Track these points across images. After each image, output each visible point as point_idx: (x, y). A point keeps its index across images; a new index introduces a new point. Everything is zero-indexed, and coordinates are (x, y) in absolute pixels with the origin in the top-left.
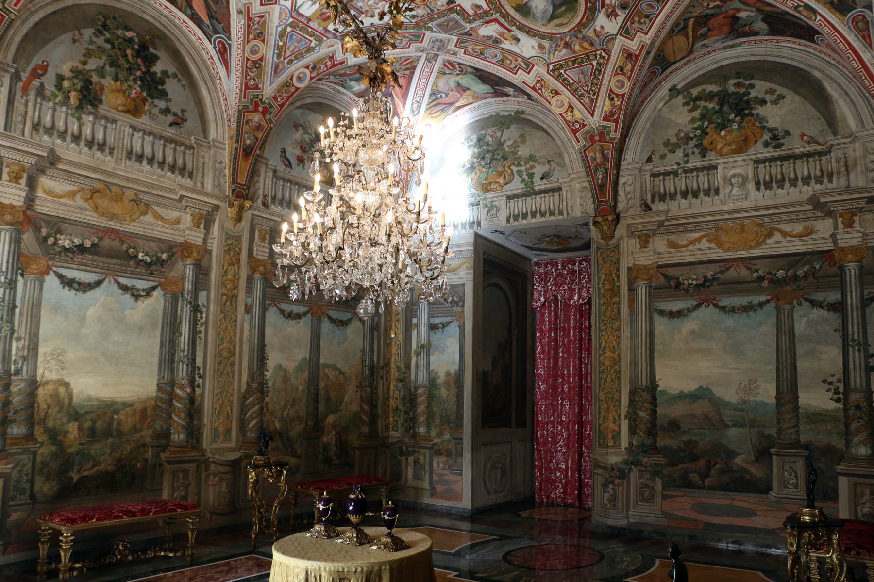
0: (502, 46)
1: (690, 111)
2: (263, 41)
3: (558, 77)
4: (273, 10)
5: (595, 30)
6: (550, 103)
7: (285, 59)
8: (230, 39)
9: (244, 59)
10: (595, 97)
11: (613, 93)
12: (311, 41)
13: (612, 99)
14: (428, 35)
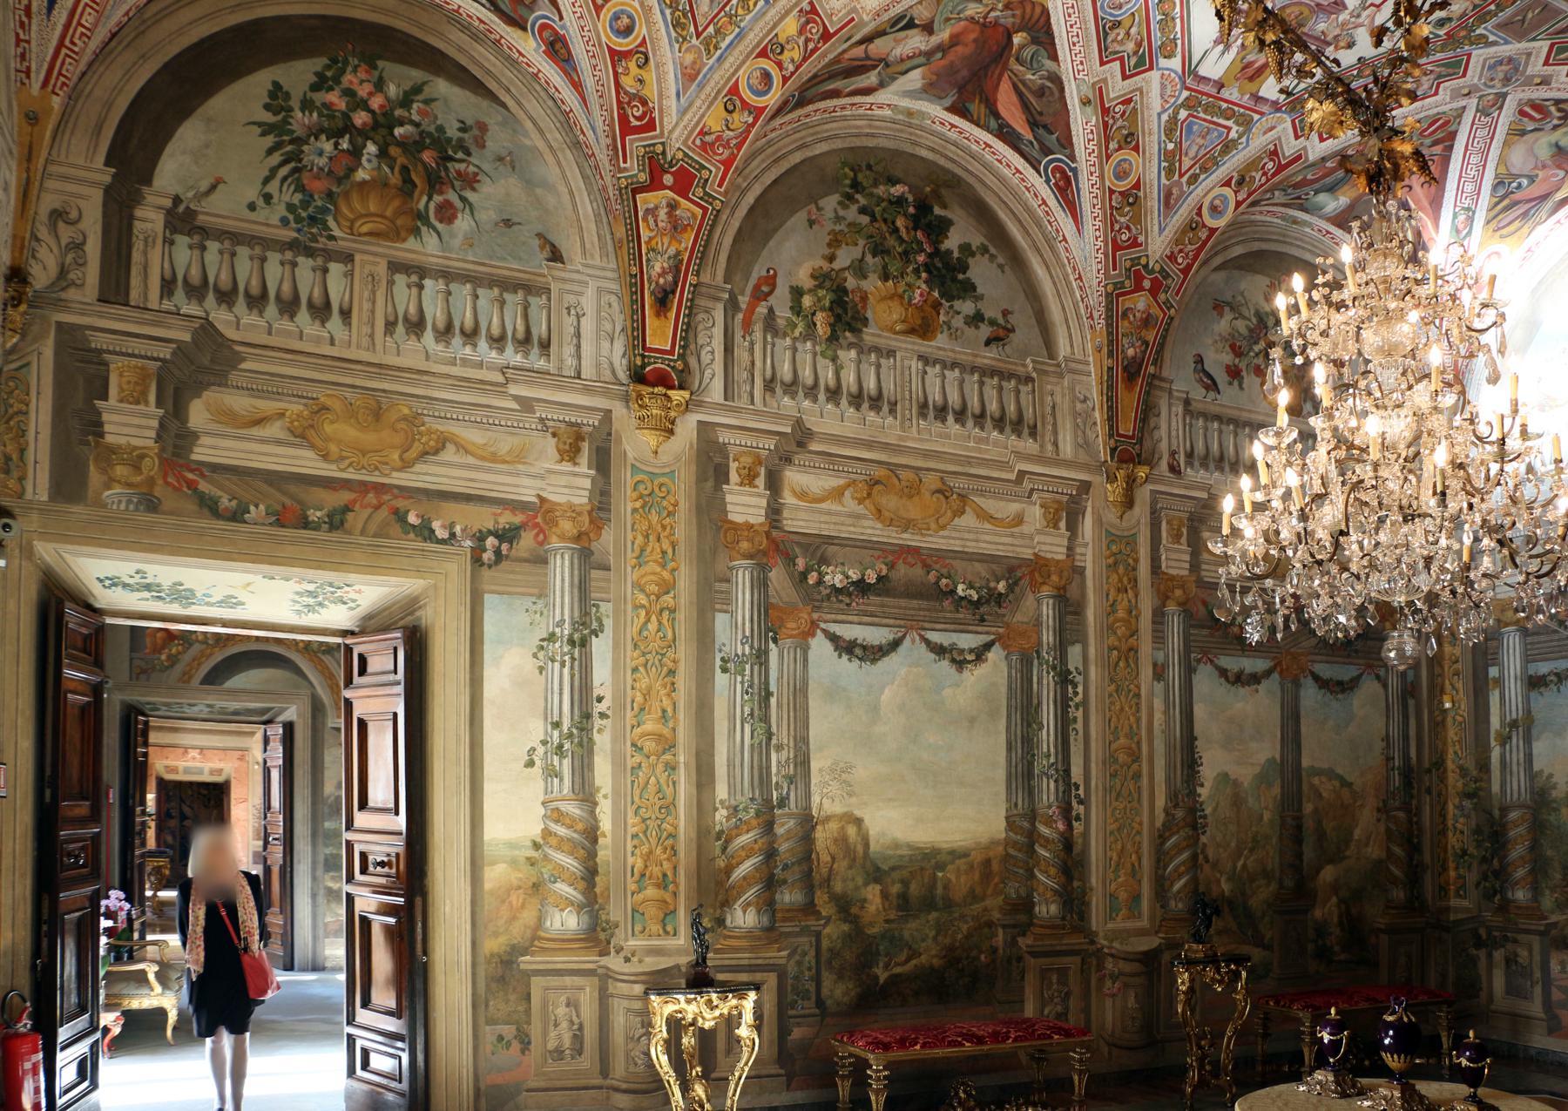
2: (1136, 149)
4: (1147, 82)
7: (1181, 176)
8: (1072, 158)
12: (1229, 129)
14: (1479, 55)
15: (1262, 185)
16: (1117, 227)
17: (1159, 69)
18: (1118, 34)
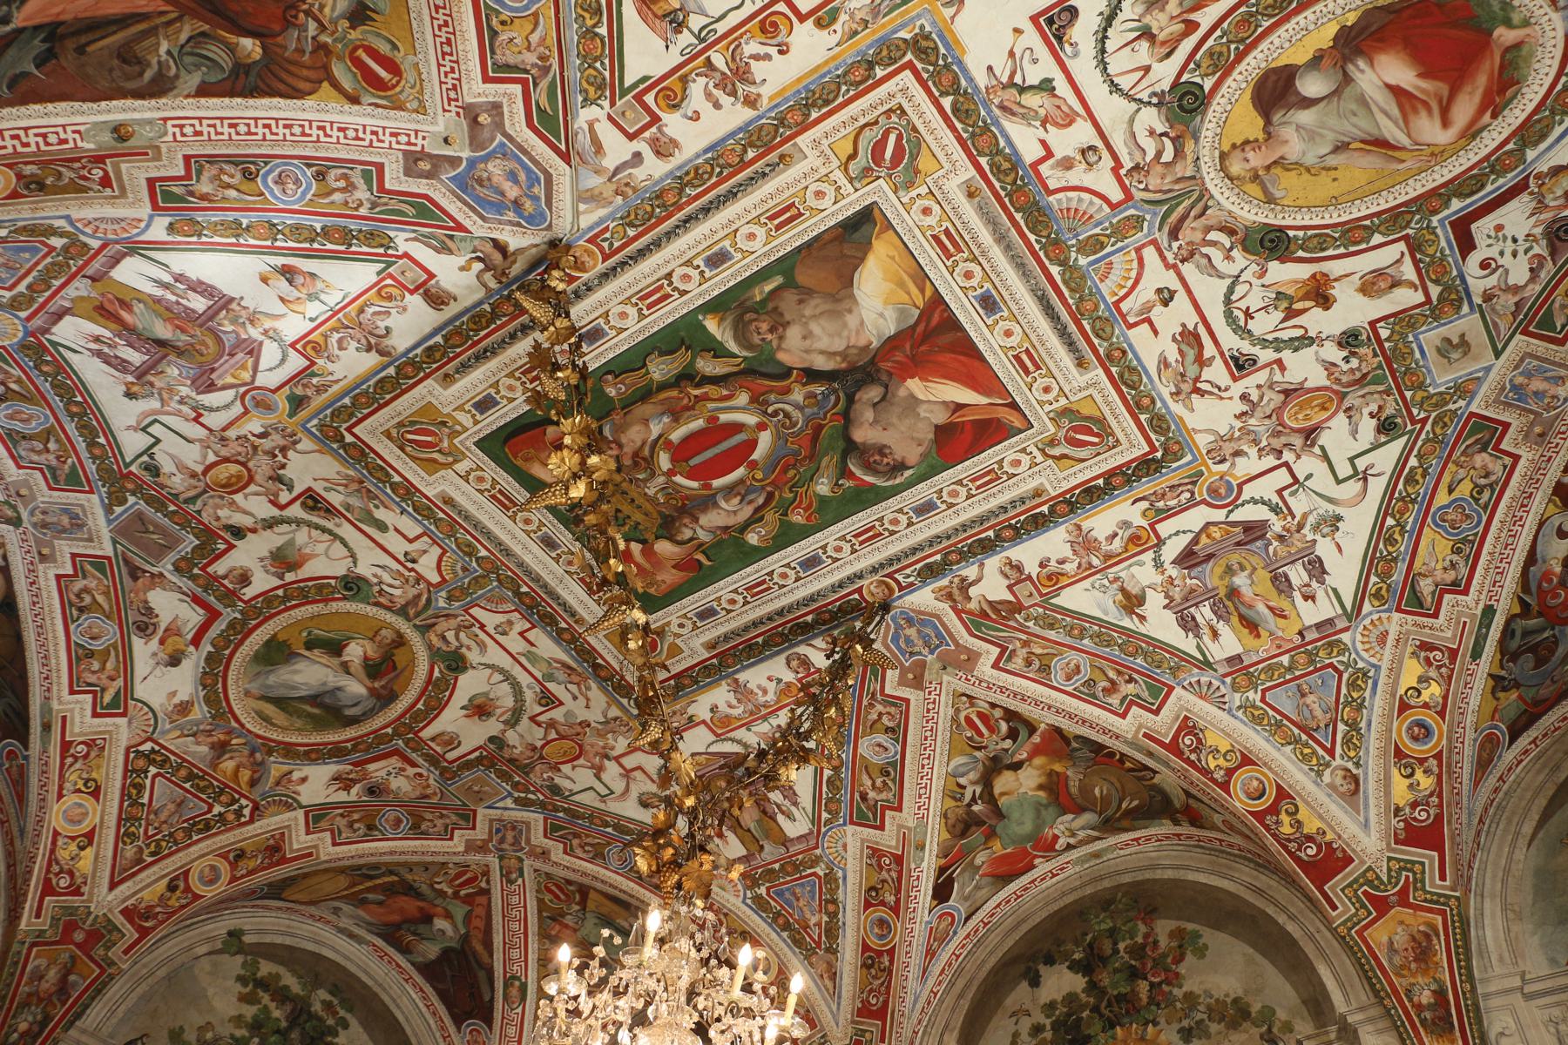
0: (137, 643)
1: (243, 999)
3: (134, 771)
6: (60, 796)
10: (150, 859)
11: (186, 880)
13: (172, 888)
17: (151, 217)
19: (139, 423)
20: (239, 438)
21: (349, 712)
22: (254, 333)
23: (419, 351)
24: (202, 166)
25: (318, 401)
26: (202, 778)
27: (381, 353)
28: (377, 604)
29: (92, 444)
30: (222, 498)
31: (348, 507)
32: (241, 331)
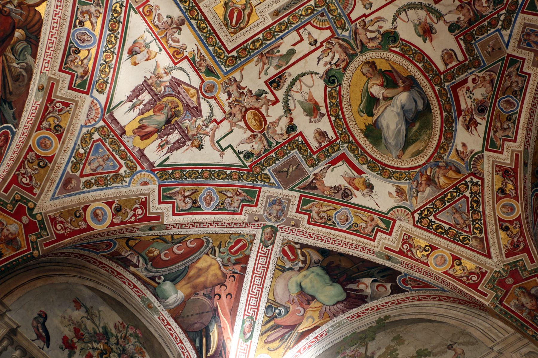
0: (354, 200)
2: (60, 137)
3: (428, 227)
4: (83, 101)
5: (457, 151)
6: (427, 264)
7: (82, 176)
8: (16, 126)
9: (25, 146)
10: (483, 235)
12: (121, 166)
13: (506, 229)
14: (266, 191)
15: (131, 222)
16: (23, 171)
17: (92, 96)
18: (76, 58)
19: (218, 151)
20: (230, 106)
21: (421, 106)
22: (166, 78)
23: (182, 6)
24: (68, 67)
25: (209, 61)
26: (446, 196)
27: (182, 23)
28: (345, 69)
29: (229, 177)
30: (268, 128)
31: (278, 66)
32: (164, 84)
